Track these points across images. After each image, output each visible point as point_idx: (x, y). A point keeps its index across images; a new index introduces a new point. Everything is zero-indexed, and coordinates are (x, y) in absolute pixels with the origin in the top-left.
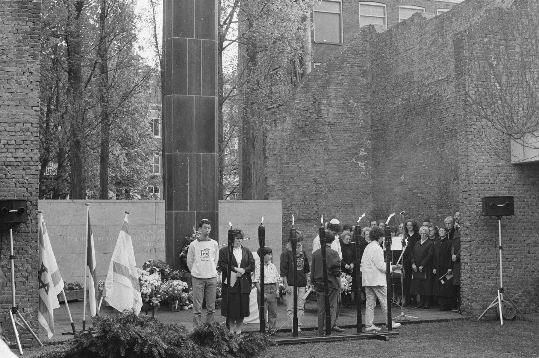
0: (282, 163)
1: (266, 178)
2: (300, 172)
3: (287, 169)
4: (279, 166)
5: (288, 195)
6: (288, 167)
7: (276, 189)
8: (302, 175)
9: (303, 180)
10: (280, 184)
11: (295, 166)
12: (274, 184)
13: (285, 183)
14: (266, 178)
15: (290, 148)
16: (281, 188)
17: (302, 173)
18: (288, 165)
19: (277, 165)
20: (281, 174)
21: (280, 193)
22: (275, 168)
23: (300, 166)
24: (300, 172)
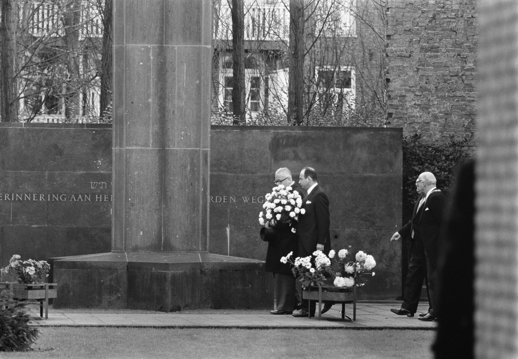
0: (422, 48)
1: (388, 80)
2: (463, 67)
3: (434, 60)
4: (417, 55)
5: (435, 118)
6: (437, 56)
7: (408, 104)
8: (467, 73)
9: (470, 85)
10: (417, 93)
11: (452, 54)
12: (404, 93)
13: (429, 91)
14: (388, 80)
15: (442, 16)
16: (419, 102)
17: (468, 70)
18: (438, 52)
19: (411, 52)
20: (421, 72)
21: (417, 112)
22: (407, 59)
23: (465, 54)
24: (463, 67)
